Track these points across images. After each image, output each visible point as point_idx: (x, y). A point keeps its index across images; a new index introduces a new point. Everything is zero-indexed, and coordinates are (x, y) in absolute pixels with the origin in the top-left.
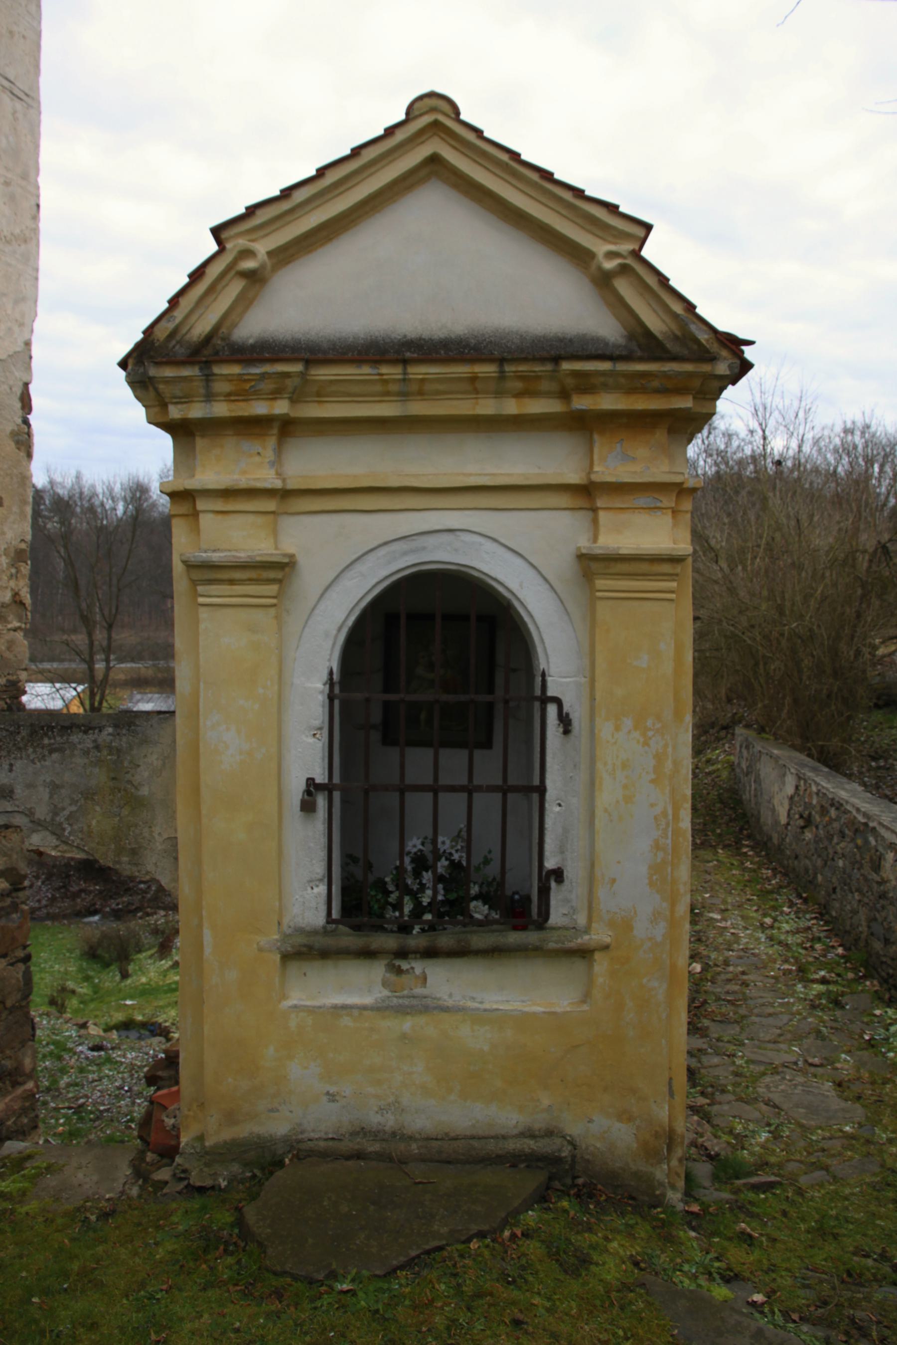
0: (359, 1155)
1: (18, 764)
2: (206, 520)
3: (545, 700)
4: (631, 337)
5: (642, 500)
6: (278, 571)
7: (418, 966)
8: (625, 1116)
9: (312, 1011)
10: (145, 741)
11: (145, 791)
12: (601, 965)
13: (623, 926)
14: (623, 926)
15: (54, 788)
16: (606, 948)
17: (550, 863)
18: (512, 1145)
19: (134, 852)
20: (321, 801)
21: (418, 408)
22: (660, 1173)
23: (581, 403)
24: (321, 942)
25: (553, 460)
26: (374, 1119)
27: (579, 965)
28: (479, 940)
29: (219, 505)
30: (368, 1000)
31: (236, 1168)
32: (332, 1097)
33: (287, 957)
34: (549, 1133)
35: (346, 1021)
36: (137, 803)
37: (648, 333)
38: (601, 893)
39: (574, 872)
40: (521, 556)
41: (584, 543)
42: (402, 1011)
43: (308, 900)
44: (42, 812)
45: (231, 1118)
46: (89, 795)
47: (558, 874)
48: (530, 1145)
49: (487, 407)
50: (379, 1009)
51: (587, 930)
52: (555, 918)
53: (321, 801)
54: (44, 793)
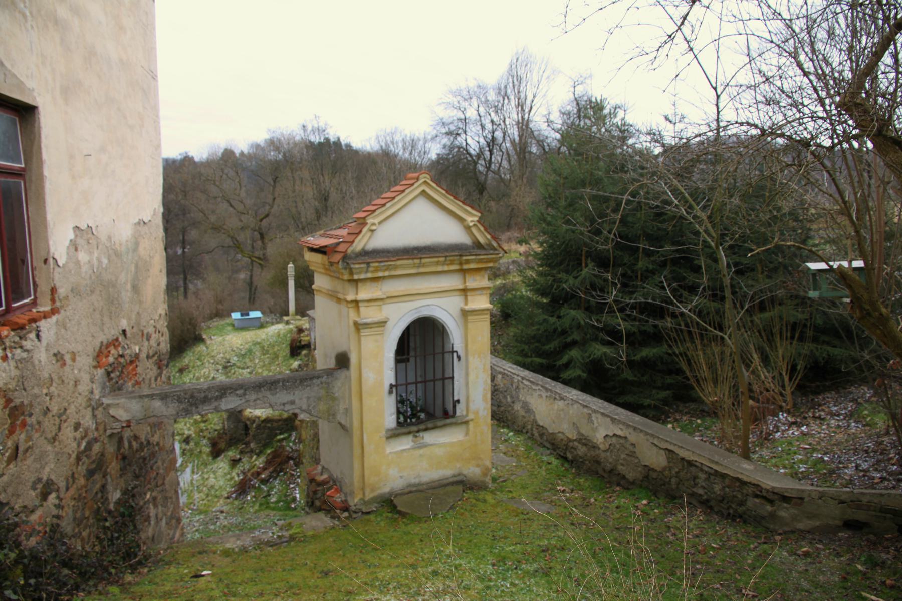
0: (411, 492)
1: (296, 392)
2: (362, 309)
3: (453, 352)
4: (474, 243)
5: (479, 292)
6: (383, 323)
7: (421, 434)
8: (478, 466)
9: (395, 453)
10: (336, 379)
11: (337, 395)
12: (471, 425)
13: (476, 413)
14: (476, 413)
15: (308, 398)
16: (472, 420)
17: (455, 398)
18: (451, 480)
19: (334, 415)
20: (394, 389)
21: (422, 270)
22: (487, 480)
23: (465, 267)
24: (397, 432)
25: (454, 282)
26: (413, 481)
27: (464, 427)
28: (440, 423)
29: (366, 304)
30: (408, 447)
31: (376, 505)
32: (401, 477)
33: (388, 438)
34: (459, 475)
35: (405, 454)
36: (334, 399)
37: (479, 243)
38: (471, 405)
39: (462, 400)
40: (445, 310)
41: (462, 305)
42: (420, 448)
43: (390, 420)
44: (304, 407)
45: (373, 490)
46: (319, 399)
47: (458, 401)
48: (455, 479)
49: (440, 269)
50: (413, 448)
51: (467, 415)
52: (458, 414)
53: (394, 389)
54: (305, 400)
